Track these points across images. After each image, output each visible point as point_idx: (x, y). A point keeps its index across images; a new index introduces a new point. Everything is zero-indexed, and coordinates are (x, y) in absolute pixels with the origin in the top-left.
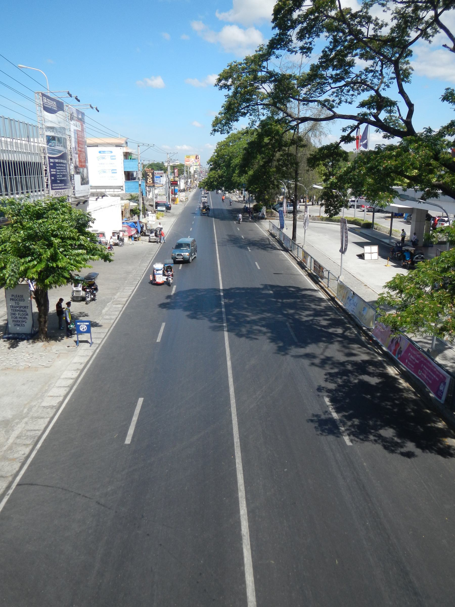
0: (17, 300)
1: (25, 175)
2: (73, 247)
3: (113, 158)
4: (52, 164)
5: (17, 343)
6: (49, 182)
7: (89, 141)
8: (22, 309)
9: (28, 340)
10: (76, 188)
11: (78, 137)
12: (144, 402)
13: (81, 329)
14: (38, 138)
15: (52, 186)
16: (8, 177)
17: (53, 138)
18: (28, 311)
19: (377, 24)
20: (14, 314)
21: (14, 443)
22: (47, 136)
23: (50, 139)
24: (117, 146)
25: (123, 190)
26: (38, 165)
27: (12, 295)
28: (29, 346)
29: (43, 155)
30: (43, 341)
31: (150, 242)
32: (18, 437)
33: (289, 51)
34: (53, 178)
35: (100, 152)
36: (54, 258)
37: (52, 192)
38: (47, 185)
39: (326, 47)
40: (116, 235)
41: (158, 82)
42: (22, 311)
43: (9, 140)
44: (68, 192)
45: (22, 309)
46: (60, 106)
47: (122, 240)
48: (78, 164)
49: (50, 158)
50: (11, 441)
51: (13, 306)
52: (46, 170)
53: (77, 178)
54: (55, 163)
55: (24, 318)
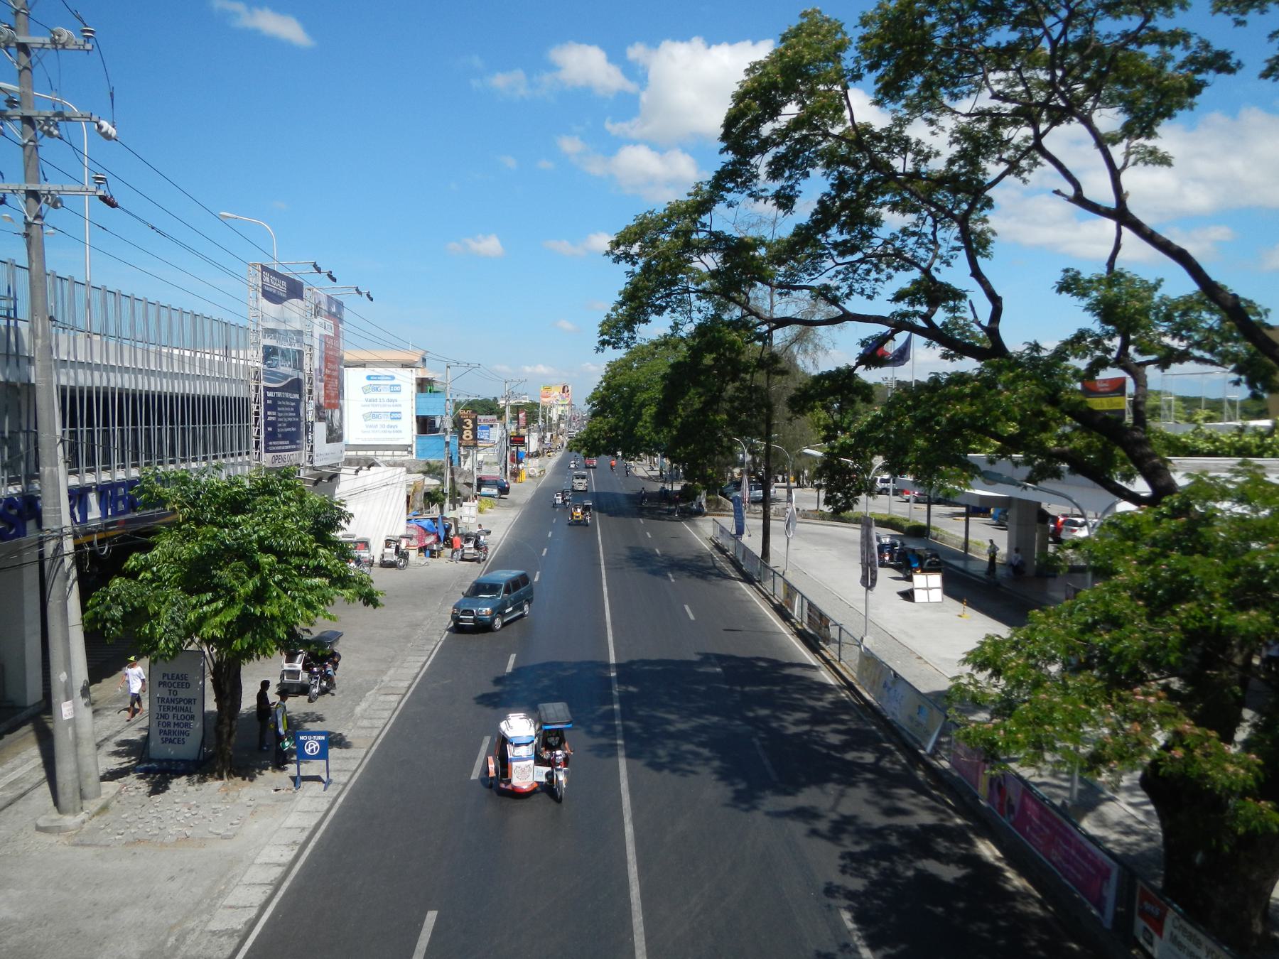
0: (172, 685)
1: (214, 422)
3: (396, 389)
4: (269, 402)
6: (262, 436)
8: (182, 704)
9: (189, 773)
10: (315, 449)
12: (439, 919)
13: (308, 751)
14: (246, 349)
15: (267, 446)
18: (195, 709)
19: (919, 153)
20: (164, 717)
22: (265, 347)
24: (405, 365)
25: (411, 452)
26: (244, 402)
27: (164, 675)
28: (191, 789)
29: (253, 384)
30: (221, 778)
31: (463, 559)
33: (750, 195)
34: (270, 429)
35: (369, 378)
36: (260, 596)
37: (267, 459)
38: (257, 443)
40: (393, 546)
41: (491, 245)
42: (182, 709)
43: (187, 353)
44: (301, 457)
45: (182, 704)
46: (295, 290)
47: (405, 556)
48: (322, 400)
49: (267, 389)
51: (163, 700)
52: (257, 413)
53: (320, 429)
54: (275, 399)
55: (187, 725)
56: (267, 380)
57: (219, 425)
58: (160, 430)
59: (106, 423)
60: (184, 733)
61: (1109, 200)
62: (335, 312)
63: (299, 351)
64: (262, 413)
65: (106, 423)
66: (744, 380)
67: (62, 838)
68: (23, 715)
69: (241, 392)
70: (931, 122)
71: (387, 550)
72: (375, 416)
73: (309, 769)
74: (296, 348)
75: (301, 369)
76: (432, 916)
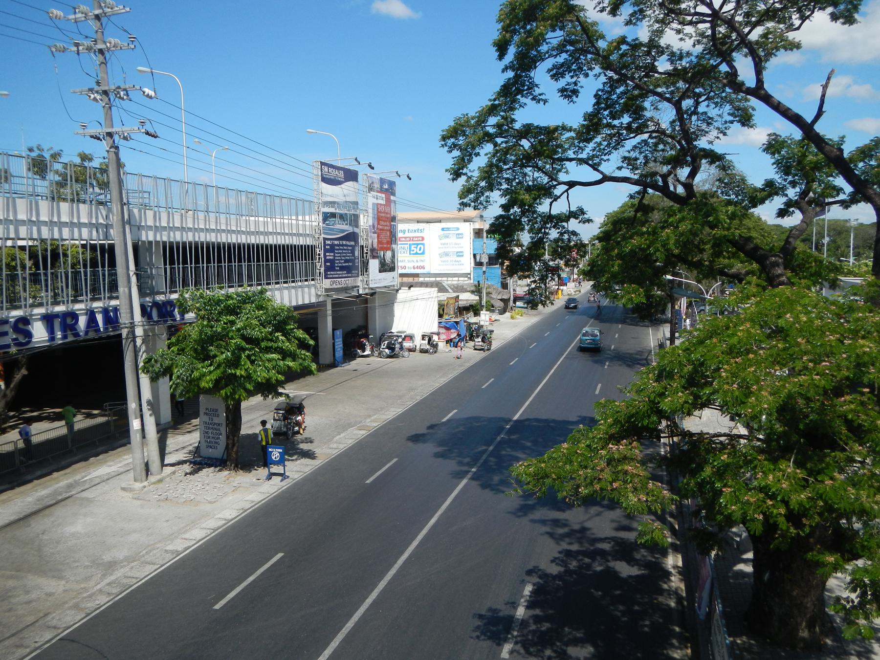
2: (268, 350)
3: (460, 236)
4: (328, 247)
5: (200, 469)
7: (400, 215)
11: (378, 212)
13: (273, 458)
14: (297, 215)
16: (244, 265)
17: (333, 215)
19: (673, 54)
20: (207, 433)
21: (100, 591)
22: (323, 213)
23: (327, 217)
25: (470, 278)
31: (475, 349)
32: (109, 584)
33: (533, 99)
35: (443, 229)
36: (235, 362)
37: (327, 284)
39: (599, 90)
40: (427, 339)
43: (261, 219)
44: (359, 281)
46: (351, 176)
47: (435, 346)
48: (375, 246)
49: (325, 239)
50: (99, 587)
54: (332, 246)
56: (324, 233)
57: (254, 264)
59: (197, 262)
60: (216, 443)
61: (751, 83)
62: (388, 188)
64: (322, 255)
65: (197, 262)
66: (563, 227)
67: (130, 495)
69: (309, 242)
70: (679, 32)
71: (424, 342)
72: (447, 254)
73: (275, 469)
74: (353, 212)
75: (357, 226)
76: (280, 555)
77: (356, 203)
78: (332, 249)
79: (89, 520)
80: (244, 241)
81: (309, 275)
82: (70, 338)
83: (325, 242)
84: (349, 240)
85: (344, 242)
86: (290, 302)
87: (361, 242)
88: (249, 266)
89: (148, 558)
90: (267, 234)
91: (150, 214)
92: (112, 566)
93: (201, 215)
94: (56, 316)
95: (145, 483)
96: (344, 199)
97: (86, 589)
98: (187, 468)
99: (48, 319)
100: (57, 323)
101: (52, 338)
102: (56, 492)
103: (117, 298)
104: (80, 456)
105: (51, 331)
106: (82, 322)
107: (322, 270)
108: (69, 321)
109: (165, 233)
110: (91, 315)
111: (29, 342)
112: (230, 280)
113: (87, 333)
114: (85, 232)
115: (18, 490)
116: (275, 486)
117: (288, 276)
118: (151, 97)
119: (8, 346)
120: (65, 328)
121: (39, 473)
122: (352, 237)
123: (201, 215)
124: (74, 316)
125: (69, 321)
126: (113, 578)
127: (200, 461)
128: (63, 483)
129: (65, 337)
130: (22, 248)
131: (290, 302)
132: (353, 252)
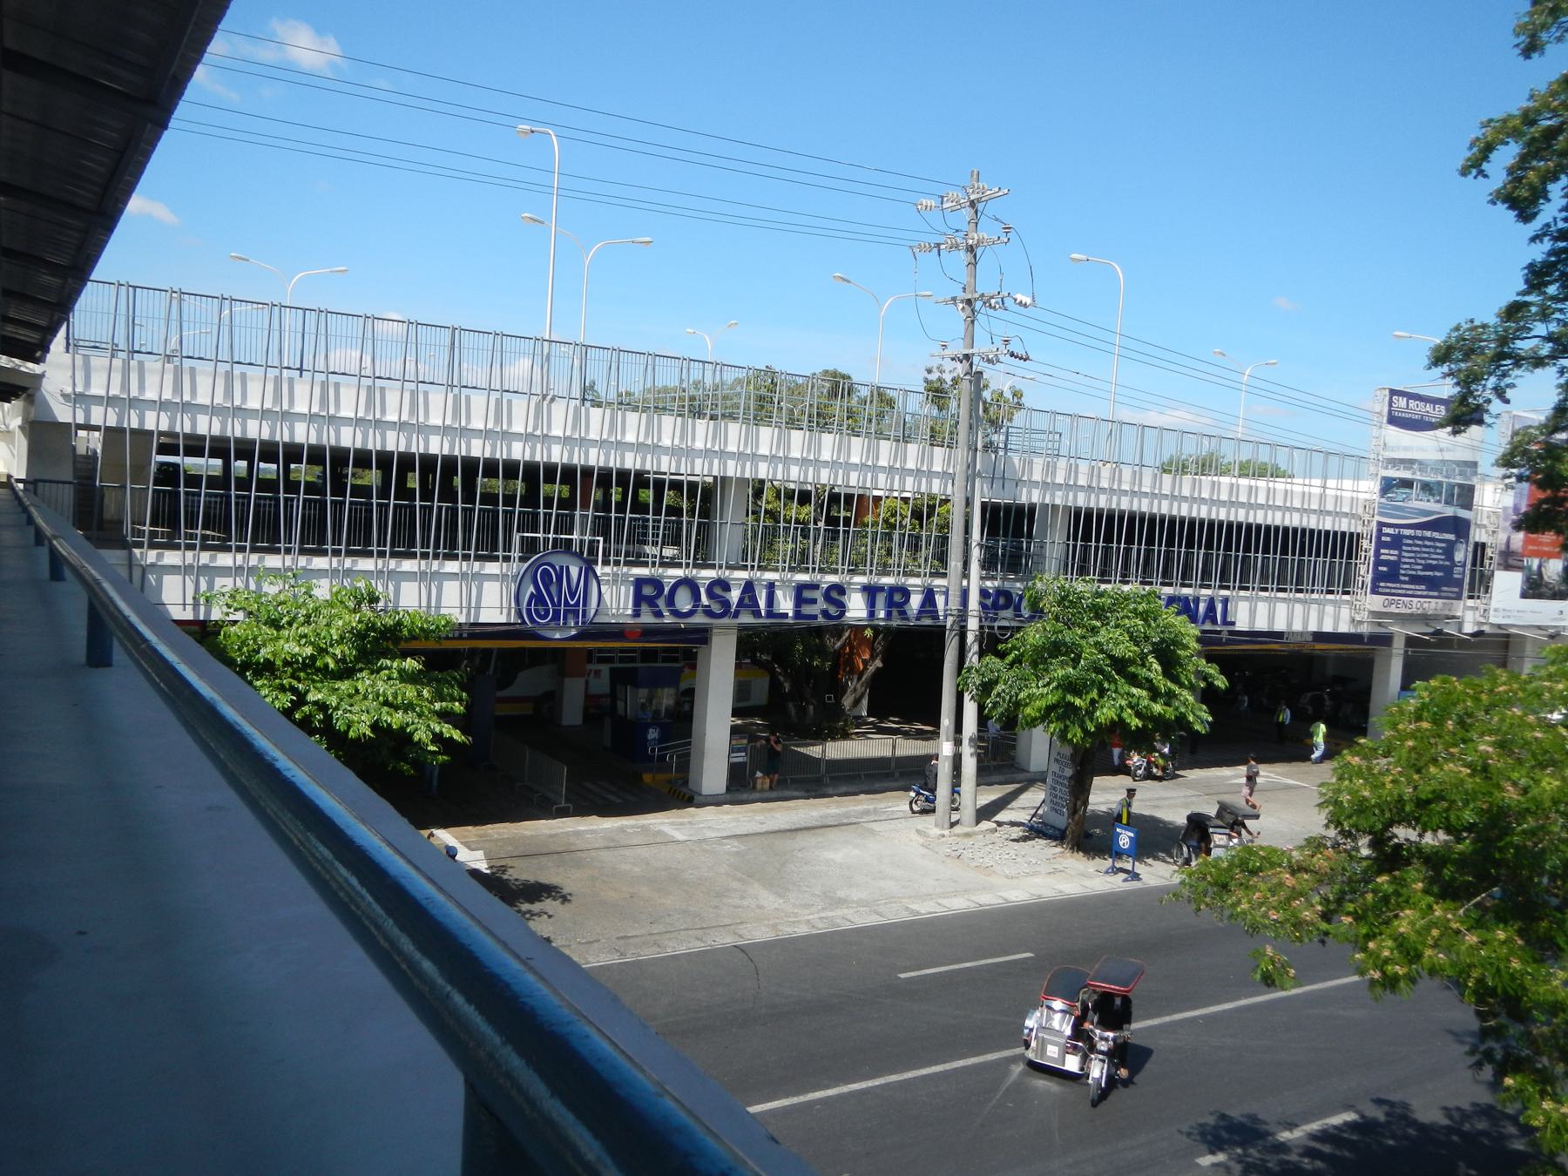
2: (1134, 680)
17: (1407, 484)
22: (1384, 478)
37: (1376, 602)
49: (1381, 525)
56: (1381, 514)
58: (1128, 551)
59: (1108, 539)
63: (1461, 486)
65: (1108, 539)
67: (921, 840)
68: (1021, 776)
74: (1459, 480)
77: (1475, 464)
78: (1397, 542)
79: (856, 852)
80: (1278, 522)
81: (1342, 582)
82: (896, 622)
83: (1379, 531)
84: (1441, 531)
85: (1428, 534)
86: (1290, 624)
87: (1478, 535)
88: (1207, 557)
89: (881, 909)
90: (1250, 506)
91: (1038, 463)
92: (840, 902)
93: (1127, 472)
94: (881, 589)
95: (946, 832)
96: (1439, 457)
97: (796, 915)
98: (1017, 832)
99: (871, 591)
100: (881, 599)
101: (872, 614)
102: (846, 815)
103: (944, 575)
104: (901, 783)
105: (871, 604)
106: (916, 601)
107: (1370, 576)
108: (897, 598)
109: (1059, 493)
110: (929, 596)
111: (843, 613)
112: (1167, 573)
113: (918, 619)
114: (910, 482)
115: (812, 801)
116: (1117, 883)
117: (1288, 579)
118: (1025, 305)
119: (815, 617)
120: (890, 603)
121: (843, 789)
122: (1460, 527)
123: (1127, 472)
124: (906, 593)
125: (897, 598)
126: (830, 914)
127: (1037, 830)
128: (860, 808)
129: (889, 615)
130: (905, 500)
131: (1290, 624)
132: (1449, 552)
